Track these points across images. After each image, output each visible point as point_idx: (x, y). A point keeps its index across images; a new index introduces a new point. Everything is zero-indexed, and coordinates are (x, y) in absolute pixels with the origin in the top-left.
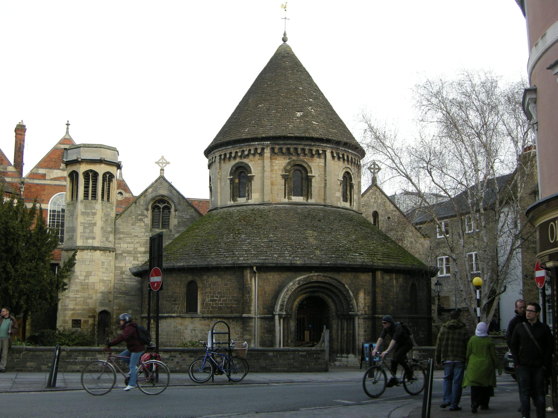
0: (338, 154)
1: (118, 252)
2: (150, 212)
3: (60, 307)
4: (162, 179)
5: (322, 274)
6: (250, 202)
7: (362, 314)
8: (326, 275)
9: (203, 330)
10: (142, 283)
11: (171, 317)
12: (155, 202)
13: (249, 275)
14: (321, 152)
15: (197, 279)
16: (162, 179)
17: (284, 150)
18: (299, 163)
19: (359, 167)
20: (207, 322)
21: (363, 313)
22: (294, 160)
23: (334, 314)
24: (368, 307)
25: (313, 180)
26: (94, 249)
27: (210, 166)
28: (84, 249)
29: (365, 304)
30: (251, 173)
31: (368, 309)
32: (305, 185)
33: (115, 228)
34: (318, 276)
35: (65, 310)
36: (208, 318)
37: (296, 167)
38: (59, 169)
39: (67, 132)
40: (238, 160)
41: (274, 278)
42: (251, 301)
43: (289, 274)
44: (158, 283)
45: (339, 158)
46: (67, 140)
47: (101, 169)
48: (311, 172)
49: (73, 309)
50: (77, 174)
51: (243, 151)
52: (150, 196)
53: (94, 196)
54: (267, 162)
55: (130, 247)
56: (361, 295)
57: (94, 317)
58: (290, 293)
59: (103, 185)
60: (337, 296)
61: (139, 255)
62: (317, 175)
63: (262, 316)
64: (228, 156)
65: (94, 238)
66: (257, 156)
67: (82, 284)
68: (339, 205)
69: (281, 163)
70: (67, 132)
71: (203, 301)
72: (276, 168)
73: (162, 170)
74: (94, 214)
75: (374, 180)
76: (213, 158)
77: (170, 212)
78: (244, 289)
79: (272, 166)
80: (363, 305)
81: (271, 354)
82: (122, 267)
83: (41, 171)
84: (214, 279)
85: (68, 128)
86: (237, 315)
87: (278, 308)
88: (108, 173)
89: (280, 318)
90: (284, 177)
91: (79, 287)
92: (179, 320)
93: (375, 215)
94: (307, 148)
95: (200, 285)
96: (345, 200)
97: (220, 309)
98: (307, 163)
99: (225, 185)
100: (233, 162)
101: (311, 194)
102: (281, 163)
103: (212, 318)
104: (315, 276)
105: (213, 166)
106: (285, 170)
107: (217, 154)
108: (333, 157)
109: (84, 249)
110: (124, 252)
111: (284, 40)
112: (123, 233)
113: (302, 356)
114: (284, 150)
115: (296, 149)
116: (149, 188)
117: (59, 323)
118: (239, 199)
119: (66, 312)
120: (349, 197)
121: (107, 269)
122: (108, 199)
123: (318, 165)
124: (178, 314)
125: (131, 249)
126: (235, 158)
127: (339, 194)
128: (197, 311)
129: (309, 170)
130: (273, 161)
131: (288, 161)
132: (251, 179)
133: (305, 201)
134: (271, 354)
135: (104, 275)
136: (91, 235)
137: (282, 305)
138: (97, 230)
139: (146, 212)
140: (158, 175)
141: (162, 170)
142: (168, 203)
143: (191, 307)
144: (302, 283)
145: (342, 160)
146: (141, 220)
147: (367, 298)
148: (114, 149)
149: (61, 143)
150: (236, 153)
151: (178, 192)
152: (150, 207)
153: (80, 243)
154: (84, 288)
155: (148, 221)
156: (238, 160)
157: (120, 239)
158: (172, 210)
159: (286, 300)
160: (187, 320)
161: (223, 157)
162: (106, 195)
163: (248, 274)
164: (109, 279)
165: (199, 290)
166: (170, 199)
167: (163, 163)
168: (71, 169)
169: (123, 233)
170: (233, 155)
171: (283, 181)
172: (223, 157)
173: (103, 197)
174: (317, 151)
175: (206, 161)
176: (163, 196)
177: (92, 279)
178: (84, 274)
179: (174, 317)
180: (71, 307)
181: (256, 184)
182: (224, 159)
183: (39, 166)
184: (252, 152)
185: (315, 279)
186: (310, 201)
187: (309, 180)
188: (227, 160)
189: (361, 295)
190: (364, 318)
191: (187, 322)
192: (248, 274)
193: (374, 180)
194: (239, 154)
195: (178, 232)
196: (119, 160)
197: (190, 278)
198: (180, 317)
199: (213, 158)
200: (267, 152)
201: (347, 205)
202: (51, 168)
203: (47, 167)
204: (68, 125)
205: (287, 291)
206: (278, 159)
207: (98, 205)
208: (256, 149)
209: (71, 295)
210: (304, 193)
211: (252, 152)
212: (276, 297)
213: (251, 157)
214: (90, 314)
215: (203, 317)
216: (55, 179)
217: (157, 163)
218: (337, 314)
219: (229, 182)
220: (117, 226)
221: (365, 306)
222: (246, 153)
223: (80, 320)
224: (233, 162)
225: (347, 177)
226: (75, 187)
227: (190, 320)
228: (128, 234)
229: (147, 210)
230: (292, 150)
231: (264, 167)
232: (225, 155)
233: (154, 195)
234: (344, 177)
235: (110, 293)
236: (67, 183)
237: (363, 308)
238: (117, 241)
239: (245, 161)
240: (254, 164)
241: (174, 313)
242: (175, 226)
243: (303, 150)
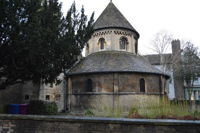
6: (128, 51)
9: (148, 99)
11: (131, 94)
49: (47, 89)
51: (125, 33)
64: (119, 33)
71: (147, 87)
76: (108, 32)
92: (137, 95)
95: (146, 80)
107: (113, 31)
111: (111, 1)
119: (43, 91)
124: (136, 93)
126: (121, 34)
128: (145, 92)
132: (128, 43)
143: (143, 90)
150: (123, 32)
156: (123, 35)
161: (116, 32)
163: (162, 77)
172: (116, 32)
179: (133, 94)
181: (130, 45)
191: (141, 96)
192: (162, 77)
197: (141, 77)
198: (138, 94)
199: (108, 32)
214: (53, 92)
215: (148, 94)
219: (119, 42)
222: (127, 34)
227: (142, 95)
231: (132, 40)
232: (118, 32)
239: (126, 36)
241: (133, 92)
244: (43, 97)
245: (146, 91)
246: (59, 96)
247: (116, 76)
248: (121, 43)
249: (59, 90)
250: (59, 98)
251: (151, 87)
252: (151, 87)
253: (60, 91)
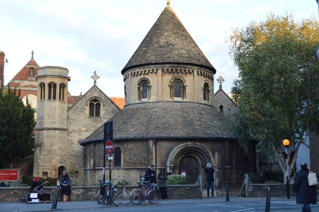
0: (201, 72)
1: (69, 131)
2: (88, 107)
3: (35, 164)
4: (95, 86)
6: (150, 101)
10: (85, 150)
12: (91, 101)
13: (151, 144)
14: (191, 71)
15: (120, 146)
16: (95, 86)
17: (170, 71)
18: (177, 78)
19: (212, 79)
20: (126, 172)
22: (175, 76)
23: (201, 166)
24: (221, 161)
25: (187, 88)
26: (56, 129)
27: (124, 80)
28: (48, 129)
30: (149, 83)
32: (182, 90)
33: (68, 117)
35: (38, 166)
36: (128, 169)
37: (177, 80)
38: (28, 80)
39: (32, 57)
40: (142, 76)
41: (166, 145)
42: (153, 158)
43: (175, 143)
44: (111, 149)
45: (201, 75)
46: (32, 62)
47: (58, 81)
49: (43, 166)
50: (44, 84)
51: (145, 71)
52: (88, 97)
53: (55, 98)
54: (160, 77)
55: (77, 128)
56: (216, 155)
57: (56, 170)
58: (175, 154)
59: (60, 91)
60: (203, 155)
61: (82, 133)
63: (159, 167)
64: (136, 74)
65: (55, 123)
66: (154, 73)
67: (48, 151)
68: (202, 102)
69: (168, 78)
70: (32, 57)
71: (125, 159)
72: (165, 81)
73: (95, 82)
74: (55, 108)
75: (221, 86)
77: (100, 107)
78: (149, 152)
79: (162, 79)
81: (170, 188)
82: (71, 140)
83: (17, 82)
84: (131, 145)
85: (33, 55)
86: (145, 167)
87: (168, 163)
88: (62, 83)
89: (170, 169)
90: (169, 86)
91: (46, 152)
93: (221, 107)
94: (183, 69)
96: (205, 99)
97: (135, 164)
99: (135, 91)
100: (139, 78)
102: (168, 78)
103: (130, 169)
104: (190, 144)
105: (127, 80)
106: (171, 82)
107: (130, 73)
108: (198, 74)
109: (48, 129)
110: (73, 131)
112: (72, 119)
113: (187, 189)
114: (170, 71)
115: (177, 70)
116: (87, 93)
117: (35, 175)
118: (143, 99)
120: (207, 97)
121: (63, 141)
122: (63, 99)
125: (77, 129)
126: (140, 75)
127: (202, 96)
129: (184, 82)
130: (163, 77)
131: (172, 77)
132: (150, 87)
133: (182, 100)
134: (170, 188)
135: (62, 145)
136: (54, 121)
137: (171, 161)
138: (57, 118)
139: (86, 107)
140: (92, 85)
141: (95, 82)
142: (99, 101)
143: (117, 162)
144: (182, 148)
145: (203, 76)
146: (83, 111)
148: (66, 69)
149: (28, 64)
151: (105, 95)
152: (88, 104)
153: (46, 126)
154: (50, 153)
155: (87, 112)
156: (142, 76)
157: (70, 123)
158: (102, 105)
159: (173, 158)
160: (115, 170)
161: (133, 74)
162: (62, 97)
164: (64, 147)
165: (122, 152)
166: (100, 99)
167: (95, 77)
168: (40, 81)
169: (72, 119)
170: (139, 73)
171: (169, 89)
172: (133, 74)
173: (60, 97)
174: (189, 71)
175: (122, 77)
176: (96, 97)
177: (55, 147)
178: (49, 144)
180: (42, 164)
182: (134, 76)
183: (16, 78)
184: (151, 72)
185: (190, 145)
186: (185, 100)
187: (184, 87)
188: (135, 76)
189: (216, 155)
192: (151, 143)
193: (221, 86)
194: (143, 73)
195: (105, 118)
196: (69, 76)
197: (116, 146)
200: (160, 71)
201: (206, 102)
202: (23, 80)
203: (20, 79)
204: (33, 53)
205: (174, 152)
206: (167, 75)
207: (57, 103)
208: (153, 70)
209: (42, 157)
210: (181, 96)
211: (151, 72)
212: (167, 156)
213: (150, 74)
215: (124, 169)
216: (25, 87)
217: (91, 77)
218: (202, 166)
219: (137, 89)
220: (69, 115)
222: (147, 72)
223: (47, 172)
224: (139, 78)
225: (206, 85)
226: (43, 94)
228: (75, 120)
229: (87, 105)
230: (174, 70)
233: (91, 96)
234: (204, 86)
235: (65, 155)
236: (38, 89)
238: (69, 125)
239: (147, 77)
240: (152, 79)
242: (103, 115)
243: (181, 70)
244: (38, 173)
245: (122, 165)
246: (77, 172)
247: (92, 145)
248: (142, 88)
249: (76, 165)
250: (76, 175)
251: (130, 159)
252: (130, 159)
253: (77, 166)
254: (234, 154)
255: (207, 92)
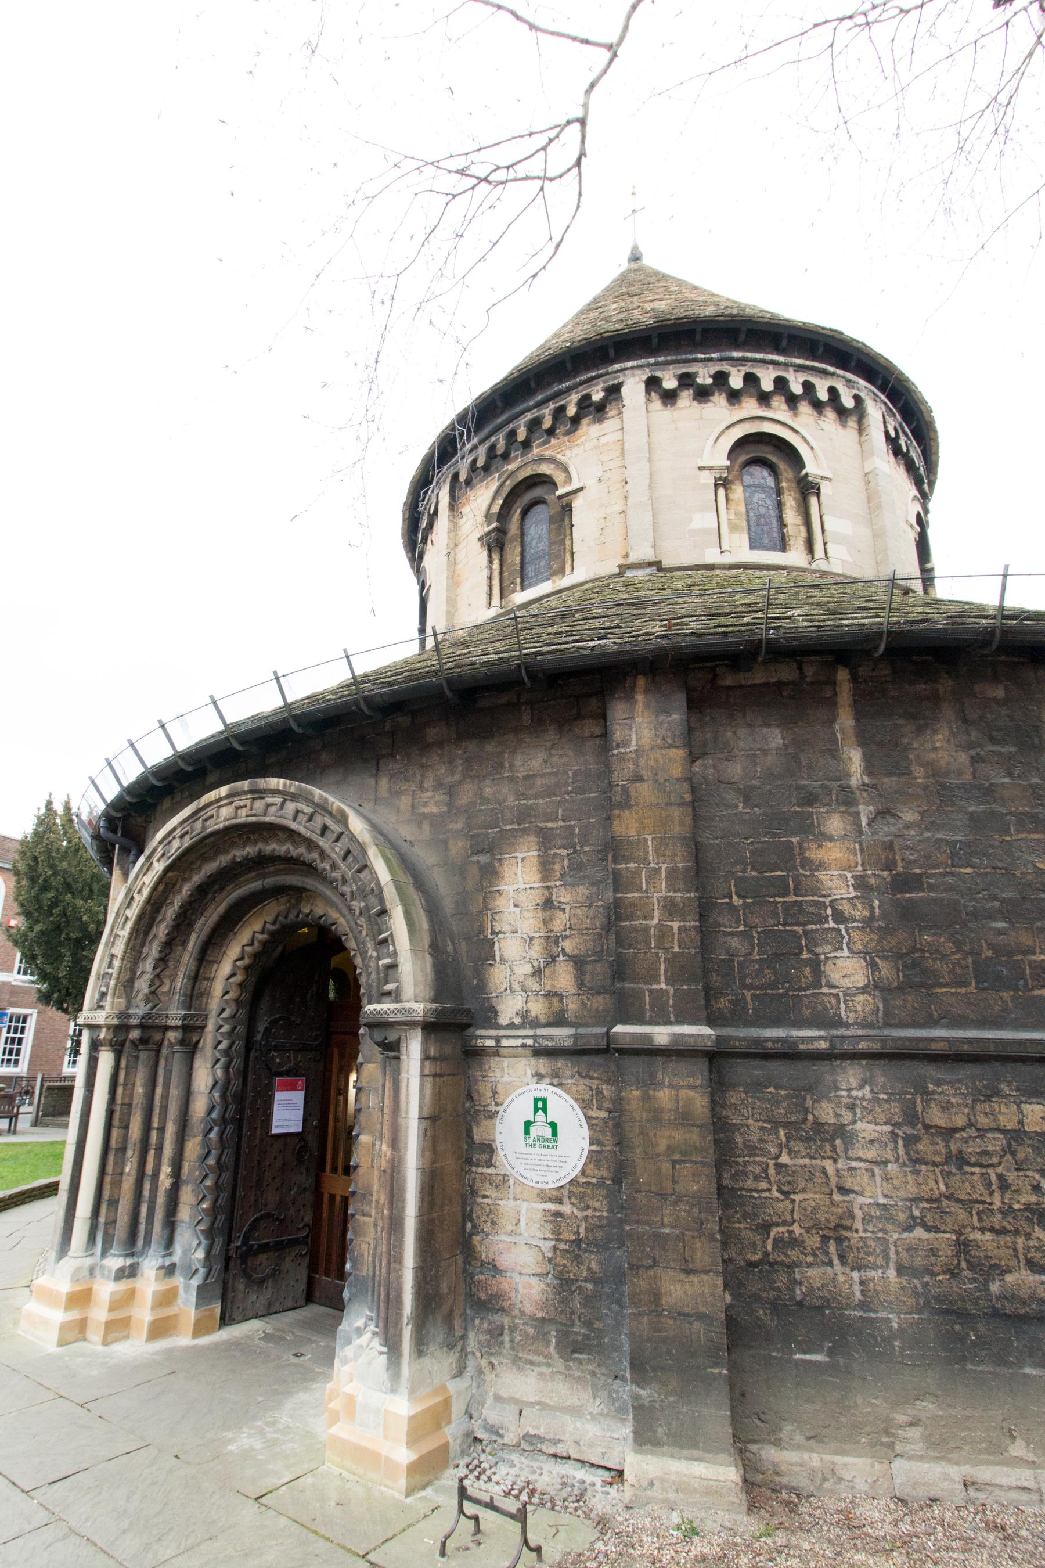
5: (245, 784)
7: (527, 1020)
8: (262, 783)
21: (537, 1008)
24: (579, 962)
29: (552, 940)
31: (580, 984)
34: (230, 795)
48: (569, 478)
62: (590, 483)
80: (536, 952)
98: (552, 460)
101: (572, 554)
123: (596, 447)
129: (559, 477)
147: (564, 896)
190: (538, 1052)
221: (552, 959)
237: (537, 973)
254: (833, 853)
255: (790, 502)
